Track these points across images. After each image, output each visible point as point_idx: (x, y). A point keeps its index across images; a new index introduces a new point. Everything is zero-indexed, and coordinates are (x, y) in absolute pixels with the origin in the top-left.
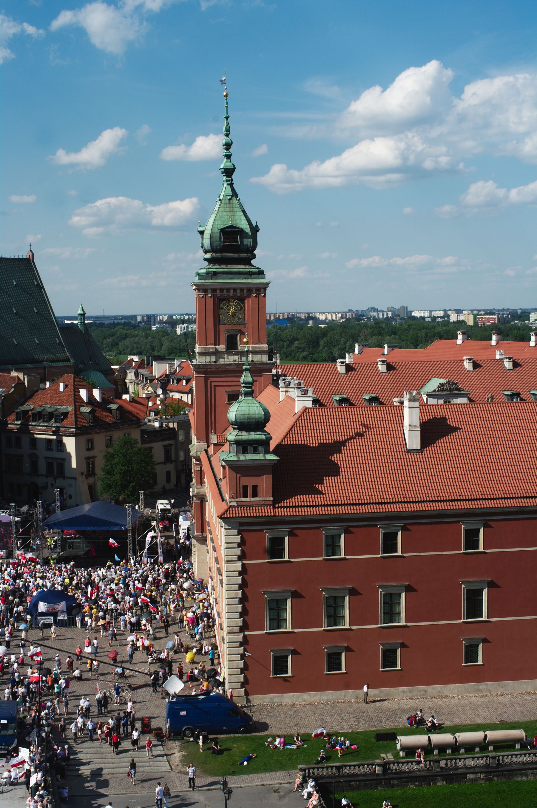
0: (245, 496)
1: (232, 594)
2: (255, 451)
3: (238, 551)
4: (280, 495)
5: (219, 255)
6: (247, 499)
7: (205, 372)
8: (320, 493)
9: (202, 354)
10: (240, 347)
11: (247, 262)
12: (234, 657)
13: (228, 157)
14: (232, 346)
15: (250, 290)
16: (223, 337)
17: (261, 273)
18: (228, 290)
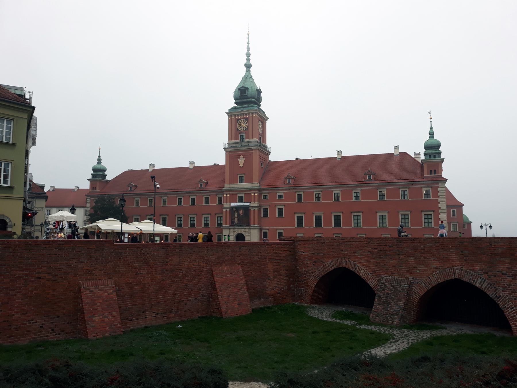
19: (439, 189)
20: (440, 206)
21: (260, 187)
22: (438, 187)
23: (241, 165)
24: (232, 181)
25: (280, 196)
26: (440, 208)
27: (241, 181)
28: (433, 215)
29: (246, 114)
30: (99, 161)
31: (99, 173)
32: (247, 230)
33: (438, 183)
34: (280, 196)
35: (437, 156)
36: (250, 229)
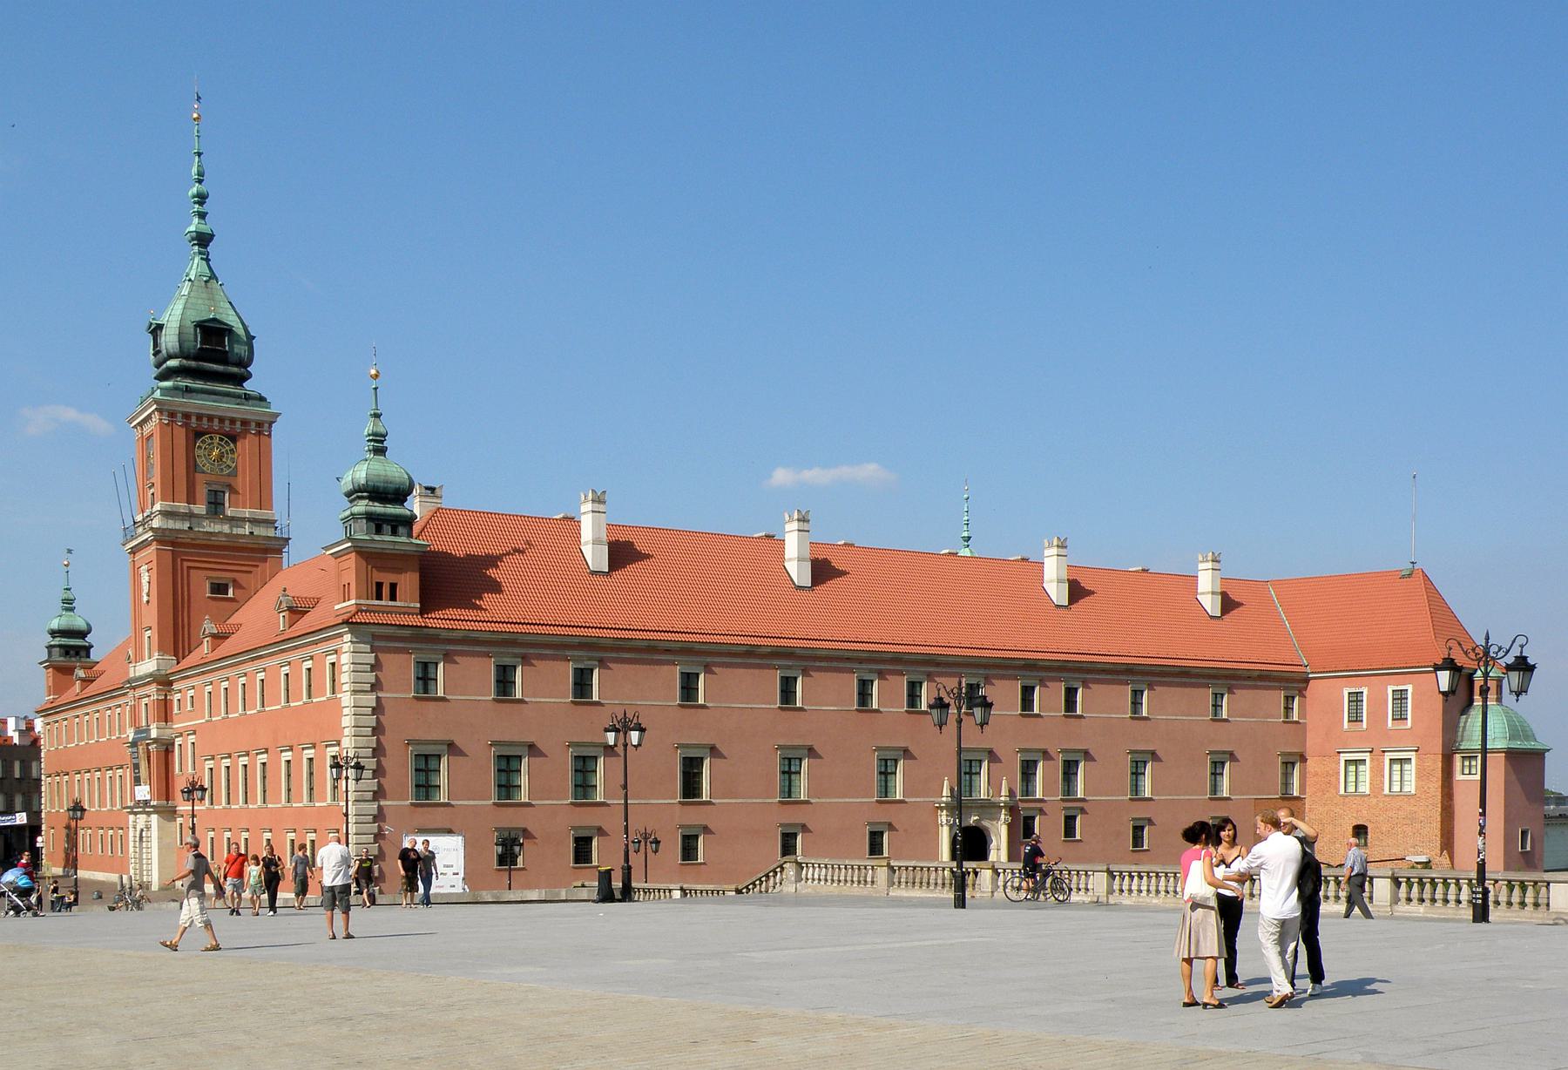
0: (379, 597)
1: (363, 741)
2: (394, 533)
3: (371, 677)
4: (430, 600)
6: (383, 603)
7: (173, 544)
8: (480, 608)
10: (229, 513)
11: (240, 380)
12: (364, 838)
14: (216, 505)
15: (245, 423)
16: (202, 491)
17: (262, 399)
18: (211, 418)
23: (145, 599)
30: (69, 605)
31: (57, 641)
33: (341, 635)
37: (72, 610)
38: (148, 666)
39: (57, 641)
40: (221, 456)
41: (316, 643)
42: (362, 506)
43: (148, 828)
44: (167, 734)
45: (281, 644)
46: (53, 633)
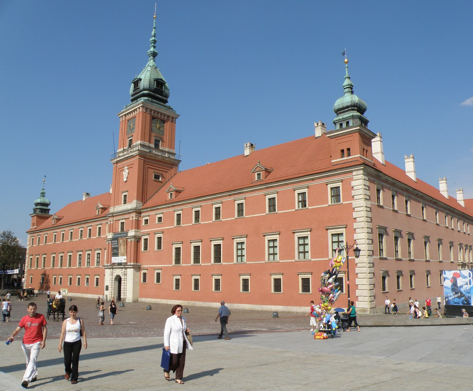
5: (153, 93)
7: (144, 157)
9: (142, 145)
10: (161, 148)
13: (154, 47)
14: (157, 146)
15: (168, 117)
19: (353, 183)
20: (355, 215)
21: (140, 208)
22: (352, 179)
23: (125, 180)
24: (117, 203)
25: (160, 219)
26: (355, 219)
27: (125, 202)
28: (344, 234)
29: (134, 111)
30: (43, 194)
31: (38, 207)
32: (123, 269)
33: (351, 172)
34: (160, 219)
35: (351, 124)
36: (127, 268)
37: (44, 196)
38: (132, 205)
39: (38, 207)
40: (159, 128)
41: (313, 180)
42: (356, 113)
43: (125, 275)
44: (138, 234)
45: (267, 185)
46: (37, 204)
